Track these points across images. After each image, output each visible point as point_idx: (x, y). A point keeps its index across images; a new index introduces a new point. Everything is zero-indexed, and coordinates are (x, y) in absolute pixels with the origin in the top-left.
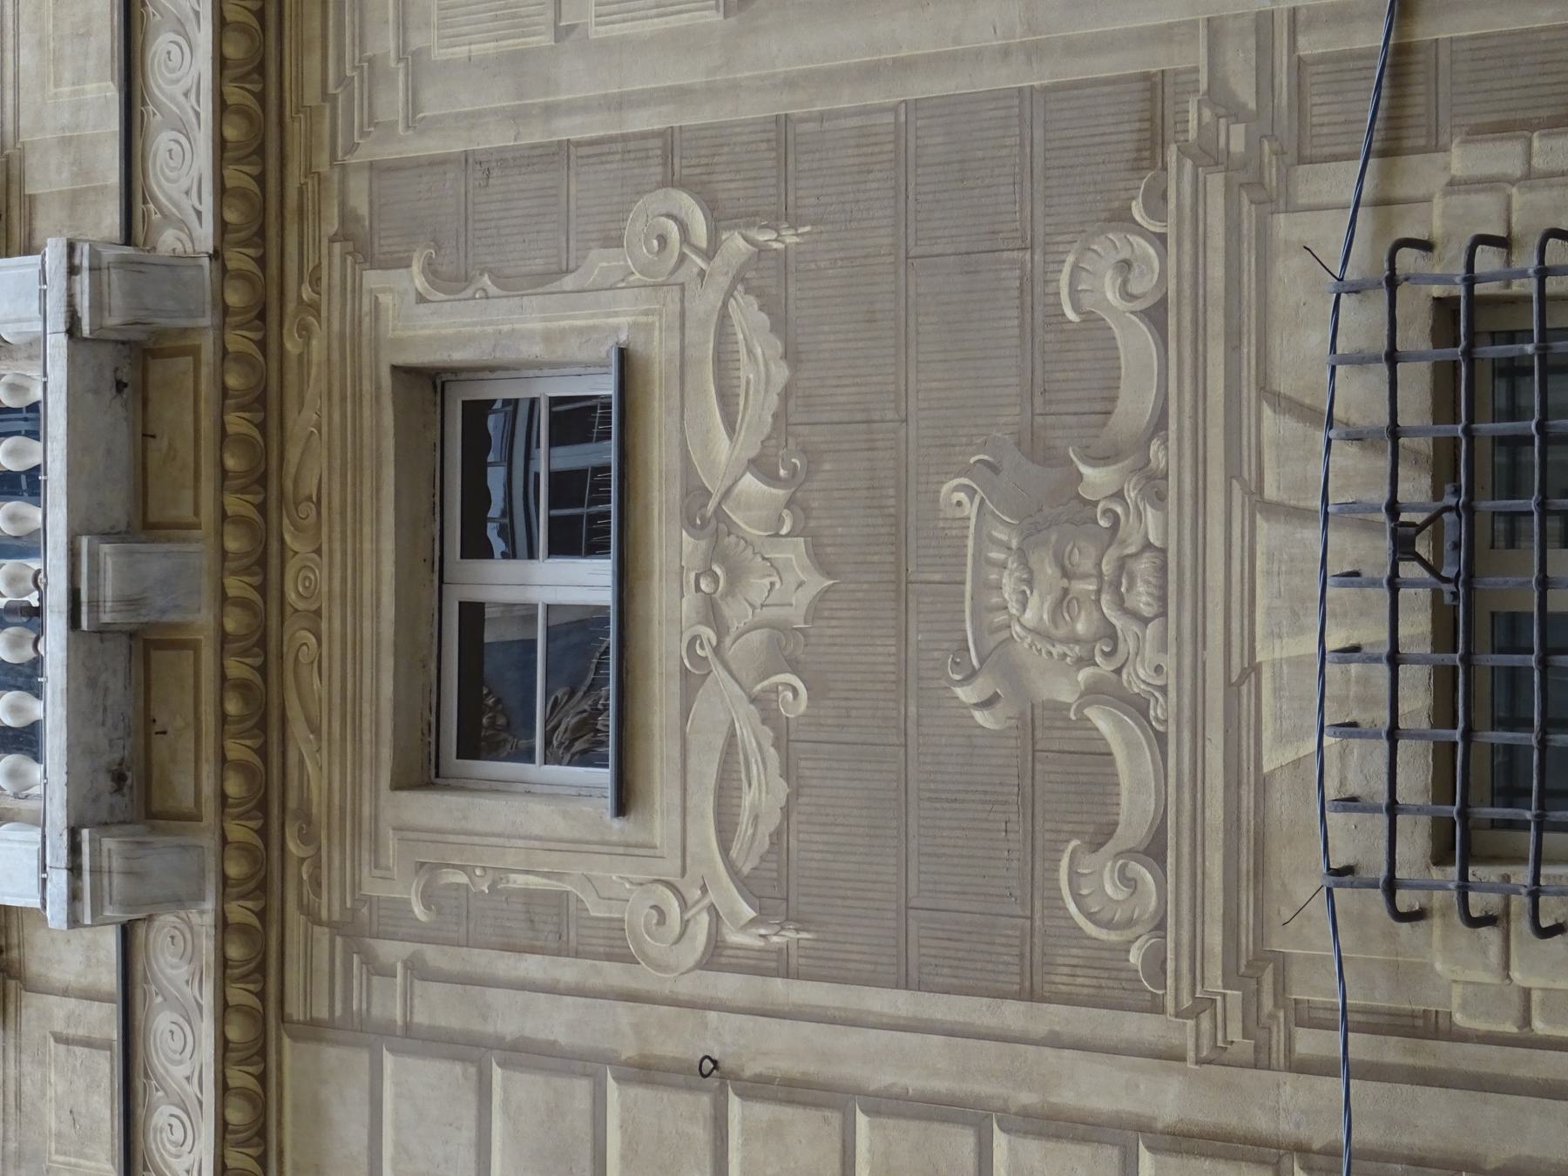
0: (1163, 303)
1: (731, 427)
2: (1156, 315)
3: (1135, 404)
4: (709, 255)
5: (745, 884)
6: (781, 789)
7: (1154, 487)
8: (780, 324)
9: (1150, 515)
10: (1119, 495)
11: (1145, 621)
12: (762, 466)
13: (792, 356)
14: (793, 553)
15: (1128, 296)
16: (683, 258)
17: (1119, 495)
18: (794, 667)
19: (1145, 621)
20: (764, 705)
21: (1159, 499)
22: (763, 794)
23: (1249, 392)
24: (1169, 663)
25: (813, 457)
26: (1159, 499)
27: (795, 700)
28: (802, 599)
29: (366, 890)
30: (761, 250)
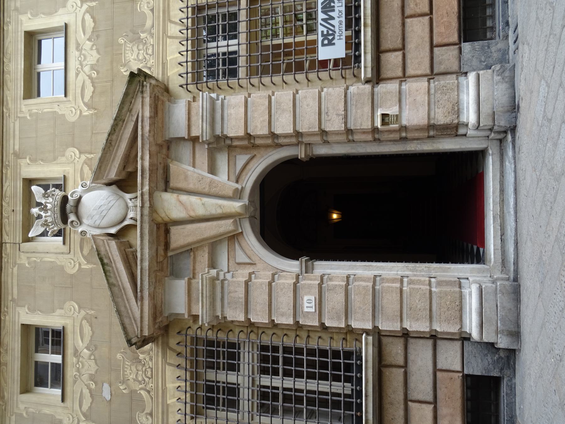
0: (153, 8)
1: (84, 34)
2: (152, 10)
3: (149, 23)
4: (81, 7)
5: (85, 104)
6: (92, 89)
7: (152, 35)
8: (93, 17)
9: (152, 40)
10: (146, 37)
11: (151, 55)
12: (89, 40)
13: (94, 21)
14: (94, 53)
15: (148, 7)
16: (76, 8)
17: (146, 37)
18: (95, 70)
19: (151, 55)
20: (90, 77)
21: (153, 37)
22: (89, 90)
23: (166, 19)
24: (154, 61)
25: (98, 37)
26: (153, 37)
27: (94, 75)
28: (96, 59)
29: (19, 115)
30: (89, 6)
